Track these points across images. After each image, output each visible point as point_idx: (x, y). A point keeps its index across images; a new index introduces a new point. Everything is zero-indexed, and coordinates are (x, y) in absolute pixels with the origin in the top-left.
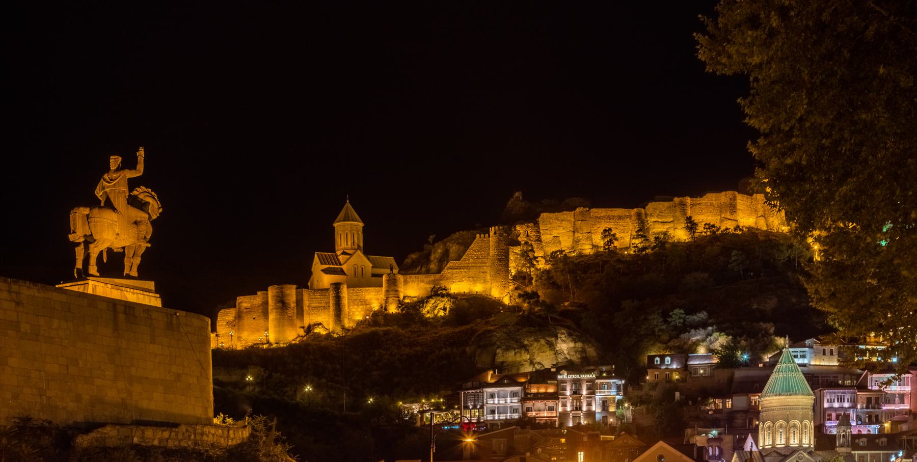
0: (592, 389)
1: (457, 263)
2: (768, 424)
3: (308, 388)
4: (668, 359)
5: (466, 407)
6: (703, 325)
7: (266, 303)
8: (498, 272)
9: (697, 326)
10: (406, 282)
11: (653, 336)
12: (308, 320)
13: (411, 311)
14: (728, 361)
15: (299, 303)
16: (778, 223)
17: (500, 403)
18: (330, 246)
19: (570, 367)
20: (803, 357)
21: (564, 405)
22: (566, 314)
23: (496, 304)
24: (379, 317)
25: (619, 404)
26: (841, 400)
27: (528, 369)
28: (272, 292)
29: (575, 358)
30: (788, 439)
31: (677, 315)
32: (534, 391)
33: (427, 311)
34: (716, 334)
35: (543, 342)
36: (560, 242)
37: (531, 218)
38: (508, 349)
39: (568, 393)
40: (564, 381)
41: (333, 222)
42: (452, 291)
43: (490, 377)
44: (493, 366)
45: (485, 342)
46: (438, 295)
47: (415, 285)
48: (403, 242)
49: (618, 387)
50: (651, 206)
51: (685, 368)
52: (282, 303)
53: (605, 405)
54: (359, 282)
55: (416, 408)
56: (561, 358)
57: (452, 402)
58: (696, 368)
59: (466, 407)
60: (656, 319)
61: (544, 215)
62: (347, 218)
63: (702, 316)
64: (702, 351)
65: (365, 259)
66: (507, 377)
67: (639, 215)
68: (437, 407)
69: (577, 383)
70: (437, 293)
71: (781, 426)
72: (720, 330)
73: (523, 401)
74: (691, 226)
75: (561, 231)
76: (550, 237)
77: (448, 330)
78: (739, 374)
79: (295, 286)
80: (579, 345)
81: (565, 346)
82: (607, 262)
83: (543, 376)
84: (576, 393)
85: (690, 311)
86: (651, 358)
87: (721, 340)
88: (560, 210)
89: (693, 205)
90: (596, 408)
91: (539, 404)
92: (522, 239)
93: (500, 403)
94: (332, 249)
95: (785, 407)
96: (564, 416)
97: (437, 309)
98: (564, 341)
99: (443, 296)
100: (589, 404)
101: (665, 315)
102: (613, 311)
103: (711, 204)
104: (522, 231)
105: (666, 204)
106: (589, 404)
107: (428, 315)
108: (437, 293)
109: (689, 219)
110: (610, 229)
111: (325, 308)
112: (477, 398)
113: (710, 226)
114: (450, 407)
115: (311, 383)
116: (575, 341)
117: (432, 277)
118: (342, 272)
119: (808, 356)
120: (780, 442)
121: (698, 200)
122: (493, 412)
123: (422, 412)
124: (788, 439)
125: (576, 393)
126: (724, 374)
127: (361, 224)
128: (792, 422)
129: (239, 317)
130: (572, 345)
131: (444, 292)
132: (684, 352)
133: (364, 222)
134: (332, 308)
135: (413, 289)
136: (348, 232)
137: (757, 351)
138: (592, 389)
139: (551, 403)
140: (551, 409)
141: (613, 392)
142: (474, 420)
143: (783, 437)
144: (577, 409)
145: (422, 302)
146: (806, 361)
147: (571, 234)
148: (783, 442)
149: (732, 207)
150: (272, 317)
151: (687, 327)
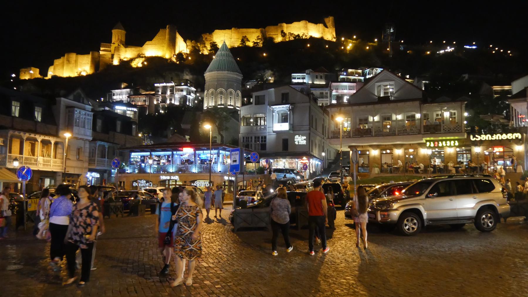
1: (150, 42)
10: (126, 51)
12: (79, 69)
15: (76, 61)
16: (330, 35)
18: (109, 41)
20: (303, 78)
33: (134, 64)
39: (160, 93)
40: (158, 87)
46: (140, 57)
61: (217, 31)
69: (165, 89)
70: (139, 56)
71: (212, 94)
74: (284, 34)
80: (195, 76)
89: (287, 27)
97: (138, 63)
98: (187, 75)
99: (142, 57)
100: (171, 100)
106: (171, 100)
109: (282, 32)
111: (88, 63)
113: (291, 34)
116: (192, 74)
117: (139, 49)
119: (306, 78)
120: (212, 104)
121: (290, 25)
127: (124, 32)
128: (219, 90)
130: (191, 76)
135: (127, 54)
143: (214, 101)
145: (132, 60)
146: (305, 81)
149: (306, 28)
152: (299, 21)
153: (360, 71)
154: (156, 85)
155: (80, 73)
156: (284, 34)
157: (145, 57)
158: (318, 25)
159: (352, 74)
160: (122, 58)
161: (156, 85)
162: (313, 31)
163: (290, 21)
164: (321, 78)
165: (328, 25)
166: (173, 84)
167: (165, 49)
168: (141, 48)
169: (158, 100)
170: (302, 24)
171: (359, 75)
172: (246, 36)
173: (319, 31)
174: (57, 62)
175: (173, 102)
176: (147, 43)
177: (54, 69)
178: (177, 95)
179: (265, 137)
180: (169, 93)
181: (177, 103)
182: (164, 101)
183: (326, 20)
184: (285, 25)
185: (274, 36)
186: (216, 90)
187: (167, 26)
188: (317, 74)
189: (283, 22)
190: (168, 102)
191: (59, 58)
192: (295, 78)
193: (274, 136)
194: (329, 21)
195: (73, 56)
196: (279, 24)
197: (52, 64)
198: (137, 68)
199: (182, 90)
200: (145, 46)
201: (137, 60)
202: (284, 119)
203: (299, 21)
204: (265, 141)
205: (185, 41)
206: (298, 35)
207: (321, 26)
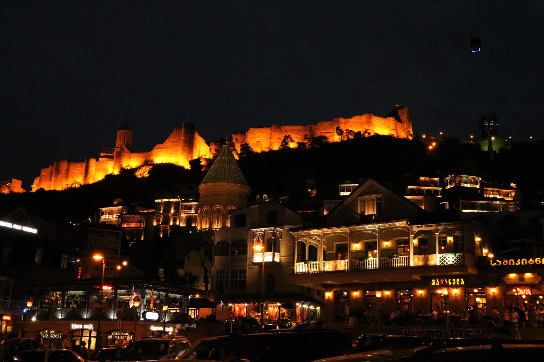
1: (161, 146)
7: (52, 172)
8: (184, 150)
10: (130, 157)
15: (68, 171)
16: (404, 132)
23: (181, 168)
24: (109, 177)
30: (211, 224)
33: (138, 174)
36: (261, 145)
39: (161, 212)
40: (159, 204)
42: (155, 162)
47: (135, 159)
50: (319, 124)
61: (252, 129)
71: (207, 212)
75: (262, 138)
76: (255, 142)
79: (67, 162)
84: (167, 211)
88: (261, 127)
89: (345, 123)
97: (144, 173)
99: (150, 165)
100: (175, 221)
103: (357, 122)
105: (329, 123)
106: (175, 221)
107: (140, 177)
108: (147, 163)
109: (338, 129)
110: (289, 136)
111: (82, 173)
113: (350, 132)
124: (211, 224)
128: (216, 207)
129: (40, 181)
131: (151, 163)
134: (84, 172)
143: (208, 222)
144: (165, 224)
147: (269, 140)
148: (207, 227)
149: (370, 123)
150: (53, 179)
152: (362, 115)
153: (436, 179)
154: (156, 201)
157: (154, 164)
158: (388, 118)
159: (426, 183)
160: (124, 165)
161: (156, 201)
162: (382, 128)
163: (348, 116)
165: (402, 118)
167: (179, 153)
168: (149, 153)
169: (158, 221)
170: (364, 118)
171: (436, 184)
172: (289, 136)
173: (389, 127)
174: (45, 172)
175: (178, 223)
176: (157, 146)
177: (40, 181)
179: (245, 272)
181: (183, 225)
182: (166, 222)
184: (342, 120)
185: (327, 135)
186: (212, 207)
192: (343, 191)
193: (256, 269)
196: (335, 119)
197: (38, 174)
198: (143, 178)
199: (190, 208)
200: (154, 151)
201: (144, 168)
203: (360, 114)
204: (245, 277)
205: (208, 143)
206: (359, 132)
207: (392, 119)
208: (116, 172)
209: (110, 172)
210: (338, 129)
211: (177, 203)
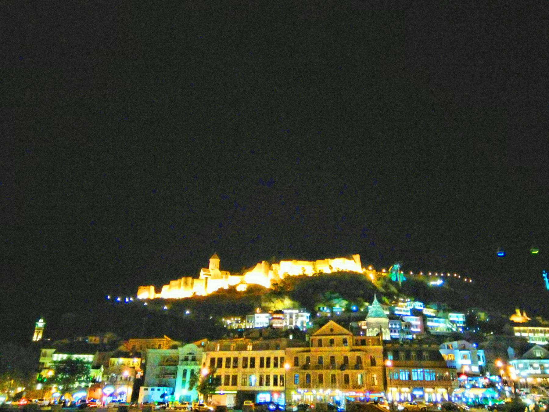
0: (297, 316)
2: (371, 329)
3: (188, 312)
4: (325, 308)
5: (248, 322)
6: (338, 298)
7: (180, 283)
9: (335, 298)
11: (319, 301)
13: (232, 290)
14: (348, 310)
15: (192, 284)
17: (260, 320)
18: (207, 266)
19: (289, 309)
21: (286, 322)
22: (288, 292)
24: (221, 290)
25: (308, 323)
26: (395, 325)
27: (274, 310)
28: (183, 279)
29: (291, 306)
31: (328, 294)
32: (275, 316)
34: (343, 301)
35: (279, 300)
37: (278, 262)
38: (266, 302)
41: (210, 258)
43: (258, 310)
44: (260, 307)
45: (258, 299)
48: (233, 266)
49: (307, 317)
50: (318, 261)
51: (332, 312)
52: (186, 283)
53: (302, 323)
54: (216, 277)
55: (229, 322)
56: (285, 307)
57: (243, 318)
58: (336, 312)
59: (248, 322)
60: (320, 296)
62: (214, 258)
63: (337, 295)
64: (337, 306)
65: (219, 271)
66: (265, 310)
67: (314, 264)
68: (237, 322)
72: (344, 299)
73: (270, 320)
74: (331, 267)
77: (245, 295)
78: (353, 315)
80: (292, 302)
81: (288, 302)
82: (303, 279)
83: (280, 312)
84: (291, 317)
85: (332, 293)
86: (319, 308)
87: (345, 303)
90: (299, 325)
91: (276, 321)
92: (274, 269)
93: (260, 320)
94: (208, 267)
95: (378, 323)
96: (286, 326)
97: (241, 288)
100: (296, 322)
101: (324, 294)
102: (306, 293)
104: (273, 265)
106: (296, 322)
109: (330, 266)
112: (253, 318)
114: (242, 322)
115: (190, 311)
118: (210, 275)
122: (258, 324)
123: (231, 324)
125: (291, 317)
126: (346, 315)
129: (170, 288)
132: (331, 307)
133: (220, 258)
136: (214, 262)
137: (360, 305)
138: (297, 316)
139: (281, 321)
140: (281, 323)
141: (306, 317)
142: (251, 327)
145: (236, 285)
151: (330, 299)
155: (195, 293)
156: (331, 267)
159: (402, 306)
163: (332, 257)
164: (386, 309)
166: (297, 311)
169: (286, 322)
174: (173, 283)
177: (170, 288)
178: (300, 319)
180: (294, 317)
182: (291, 323)
183: (354, 256)
184: (329, 260)
187: (263, 262)
188: (385, 307)
189: (328, 258)
190: (294, 324)
191: (176, 279)
194: (357, 257)
195: (190, 279)
197: (168, 284)
199: (302, 316)
202: (464, 357)
207: (352, 261)
208: (226, 287)
209: (220, 287)
210: (330, 266)
211: (297, 313)
